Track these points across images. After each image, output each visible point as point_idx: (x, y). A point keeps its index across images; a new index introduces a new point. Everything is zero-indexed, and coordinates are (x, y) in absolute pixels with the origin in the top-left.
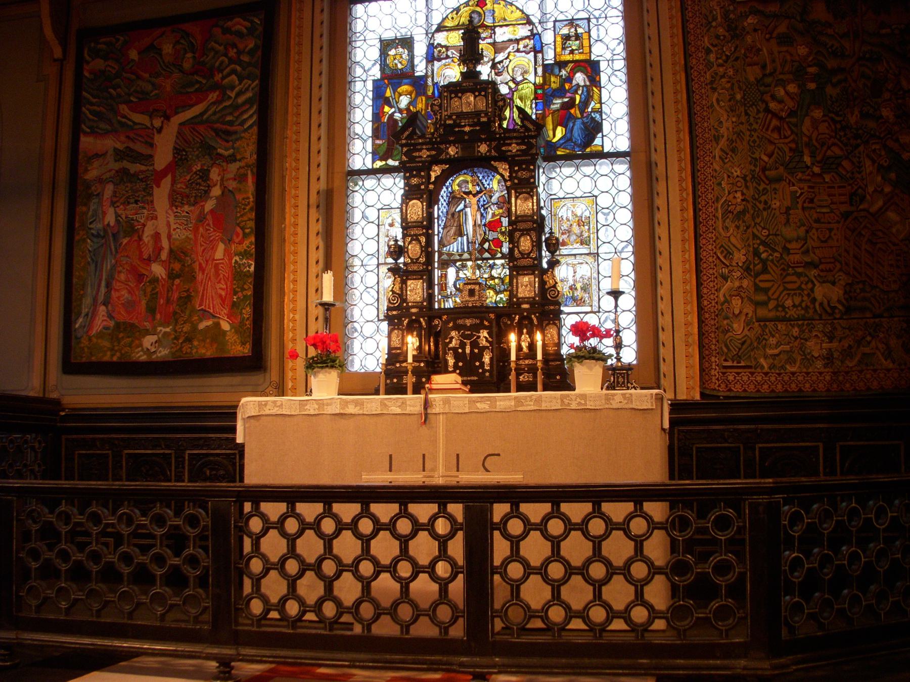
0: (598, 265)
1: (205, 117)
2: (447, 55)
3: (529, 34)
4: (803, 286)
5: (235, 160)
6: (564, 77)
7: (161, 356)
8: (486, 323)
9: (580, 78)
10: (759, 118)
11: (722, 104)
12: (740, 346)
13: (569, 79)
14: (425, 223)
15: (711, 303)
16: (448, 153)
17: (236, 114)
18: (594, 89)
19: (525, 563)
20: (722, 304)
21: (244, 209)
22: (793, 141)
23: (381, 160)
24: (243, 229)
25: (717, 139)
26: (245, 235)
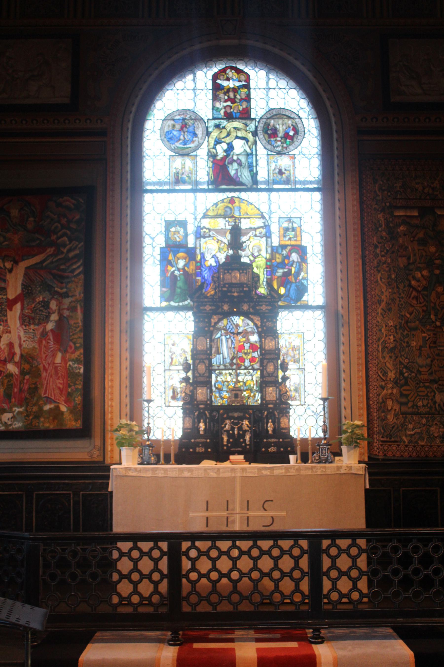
0: (305, 376)
1: (45, 264)
2: (209, 234)
3: (263, 225)
4: (429, 394)
6: (284, 255)
7: (16, 428)
8: (247, 416)
9: (294, 257)
10: (405, 290)
11: (383, 280)
12: (391, 429)
13: (288, 257)
14: (208, 352)
15: (374, 403)
16: (223, 309)
17: (68, 265)
18: (304, 264)
19: (339, 570)
20: (381, 403)
21: (75, 330)
22: (425, 305)
23: (166, 300)
24: (75, 343)
25: (380, 302)
26: (76, 348)
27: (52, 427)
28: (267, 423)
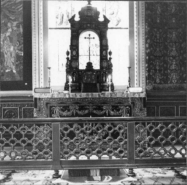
1: (5, 6)
5: (16, 21)
17: (15, 6)
27: (10, 80)
28: (103, 77)
